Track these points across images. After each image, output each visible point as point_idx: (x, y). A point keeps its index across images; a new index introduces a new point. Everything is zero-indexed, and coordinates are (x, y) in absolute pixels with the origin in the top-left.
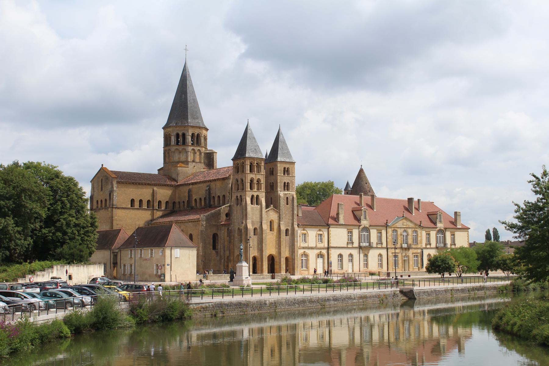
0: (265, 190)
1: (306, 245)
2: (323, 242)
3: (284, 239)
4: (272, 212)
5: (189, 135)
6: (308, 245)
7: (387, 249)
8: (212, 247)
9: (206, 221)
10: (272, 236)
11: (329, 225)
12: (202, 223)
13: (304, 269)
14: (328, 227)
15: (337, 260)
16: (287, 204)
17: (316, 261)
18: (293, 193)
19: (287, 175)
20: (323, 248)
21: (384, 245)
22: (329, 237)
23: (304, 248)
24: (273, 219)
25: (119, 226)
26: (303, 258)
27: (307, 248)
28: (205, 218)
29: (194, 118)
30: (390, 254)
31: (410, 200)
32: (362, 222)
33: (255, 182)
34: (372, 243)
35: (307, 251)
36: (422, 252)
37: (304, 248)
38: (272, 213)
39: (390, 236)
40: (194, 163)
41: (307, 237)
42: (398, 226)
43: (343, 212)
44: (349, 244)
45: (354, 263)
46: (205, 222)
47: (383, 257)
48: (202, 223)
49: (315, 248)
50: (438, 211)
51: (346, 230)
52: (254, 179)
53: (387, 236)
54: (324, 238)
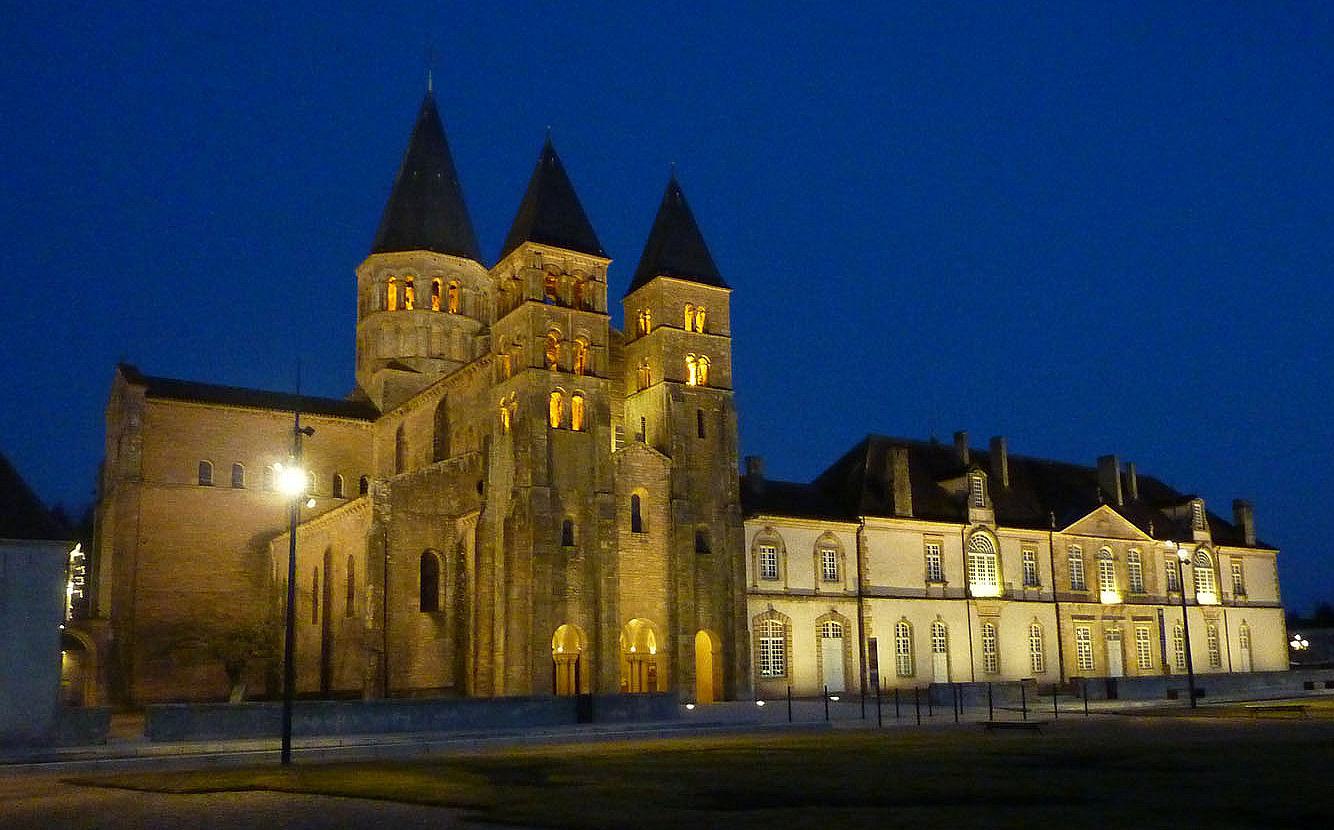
1: (778, 587)
4: (638, 459)
8: (417, 602)
12: (377, 507)
23: (769, 595)
36: (1161, 617)
37: (769, 595)
40: (439, 364)
41: (781, 557)
44: (933, 585)
45: (952, 654)
46: (387, 507)
48: (377, 507)
49: (815, 595)
53: (1055, 565)
54: (844, 565)
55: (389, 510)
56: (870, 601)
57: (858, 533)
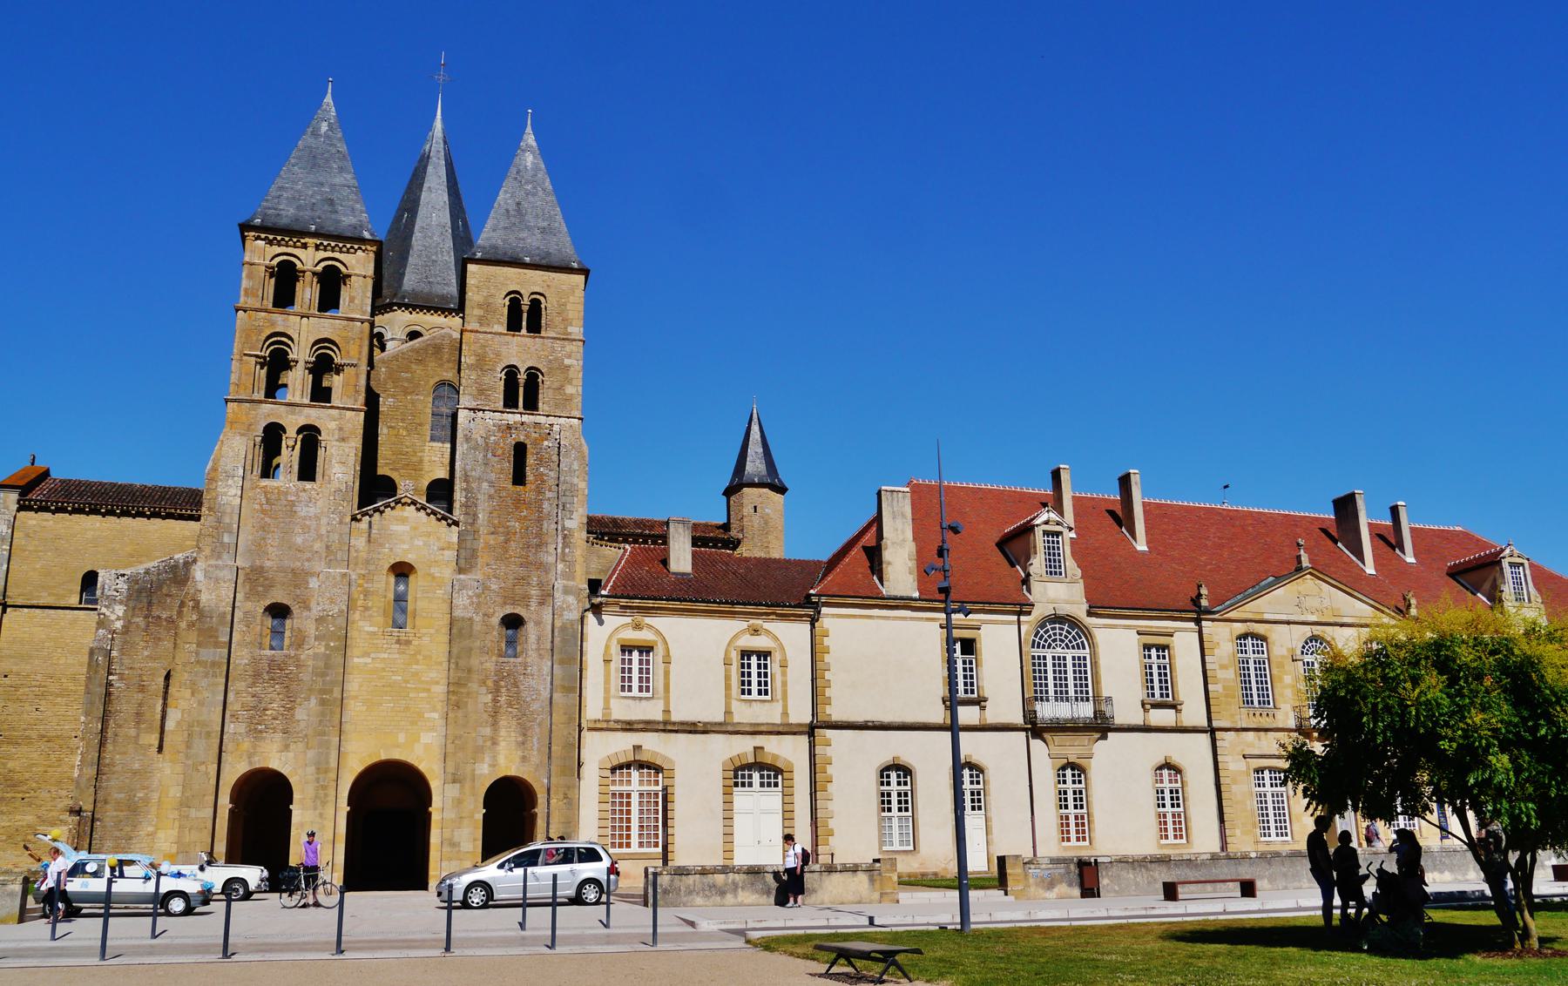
0: (366, 404)
1: (653, 712)
2: (779, 695)
3: (469, 671)
4: (404, 520)
5: (392, 339)
6: (667, 712)
7: (1212, 731)
9: (126, 605)
10: (404, 653)
11: (814, 599)
13: (635, 848)
14: (811, 612)
15: (874, 800)
16: (519, 478)
17: (728, 803)
18: (562, 420)
19: (524, 331)
20: (785, 730)
21: (1194, 713)
22: (819, 665)
23: (629, 727)
24: (409, 558)
25: (7, 682)
26: (625, 788)
27: (657, 731)
28: (122, 585)
29: (429, 282)
30: (1233, 764)
31: (1345, 506)
32: (1035, 586)
33: (301, 353)
34: (1109, 699)
35: (653, 744)
37: (629, 727)
38: (407, 528)
39: (1223, 667)
42: (1267, 617)
43: (909, 534)
45: (993, 814)
46: (120, 610)
47: (1189, 775)
50: (1502, 551)
51: (938, 624)
52: (292, 340)
54: (784, 674)
55: (121, 614)
56: (829, 733)
57: (813, 626)
